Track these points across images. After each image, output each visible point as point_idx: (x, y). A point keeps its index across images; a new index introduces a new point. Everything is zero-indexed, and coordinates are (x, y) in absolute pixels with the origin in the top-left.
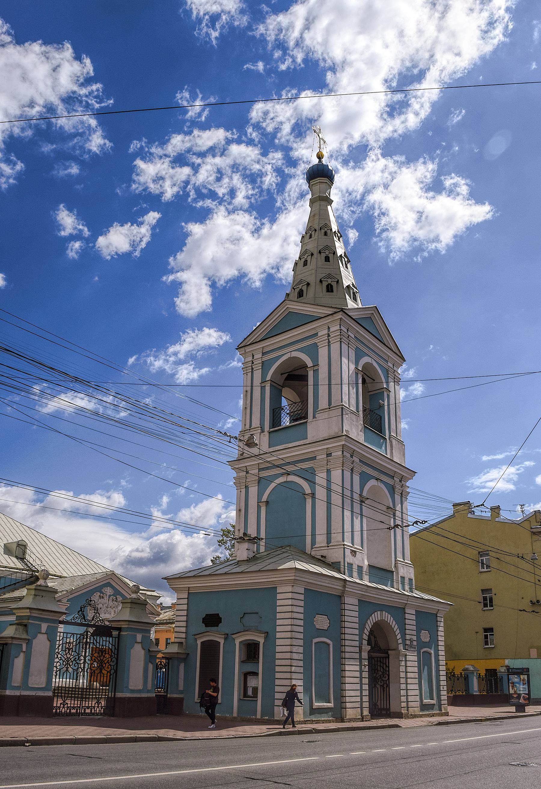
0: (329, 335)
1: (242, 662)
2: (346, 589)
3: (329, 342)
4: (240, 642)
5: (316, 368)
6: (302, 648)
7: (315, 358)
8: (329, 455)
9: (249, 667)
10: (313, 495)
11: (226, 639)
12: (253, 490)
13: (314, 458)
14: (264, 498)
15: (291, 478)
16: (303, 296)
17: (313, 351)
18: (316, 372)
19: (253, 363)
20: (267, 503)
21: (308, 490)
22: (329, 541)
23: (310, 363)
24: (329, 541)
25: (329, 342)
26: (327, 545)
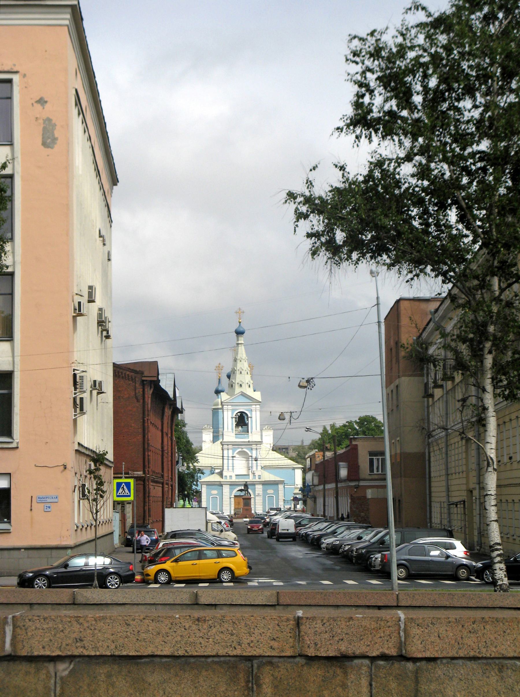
7: (251, 414)
23: (249, 416)
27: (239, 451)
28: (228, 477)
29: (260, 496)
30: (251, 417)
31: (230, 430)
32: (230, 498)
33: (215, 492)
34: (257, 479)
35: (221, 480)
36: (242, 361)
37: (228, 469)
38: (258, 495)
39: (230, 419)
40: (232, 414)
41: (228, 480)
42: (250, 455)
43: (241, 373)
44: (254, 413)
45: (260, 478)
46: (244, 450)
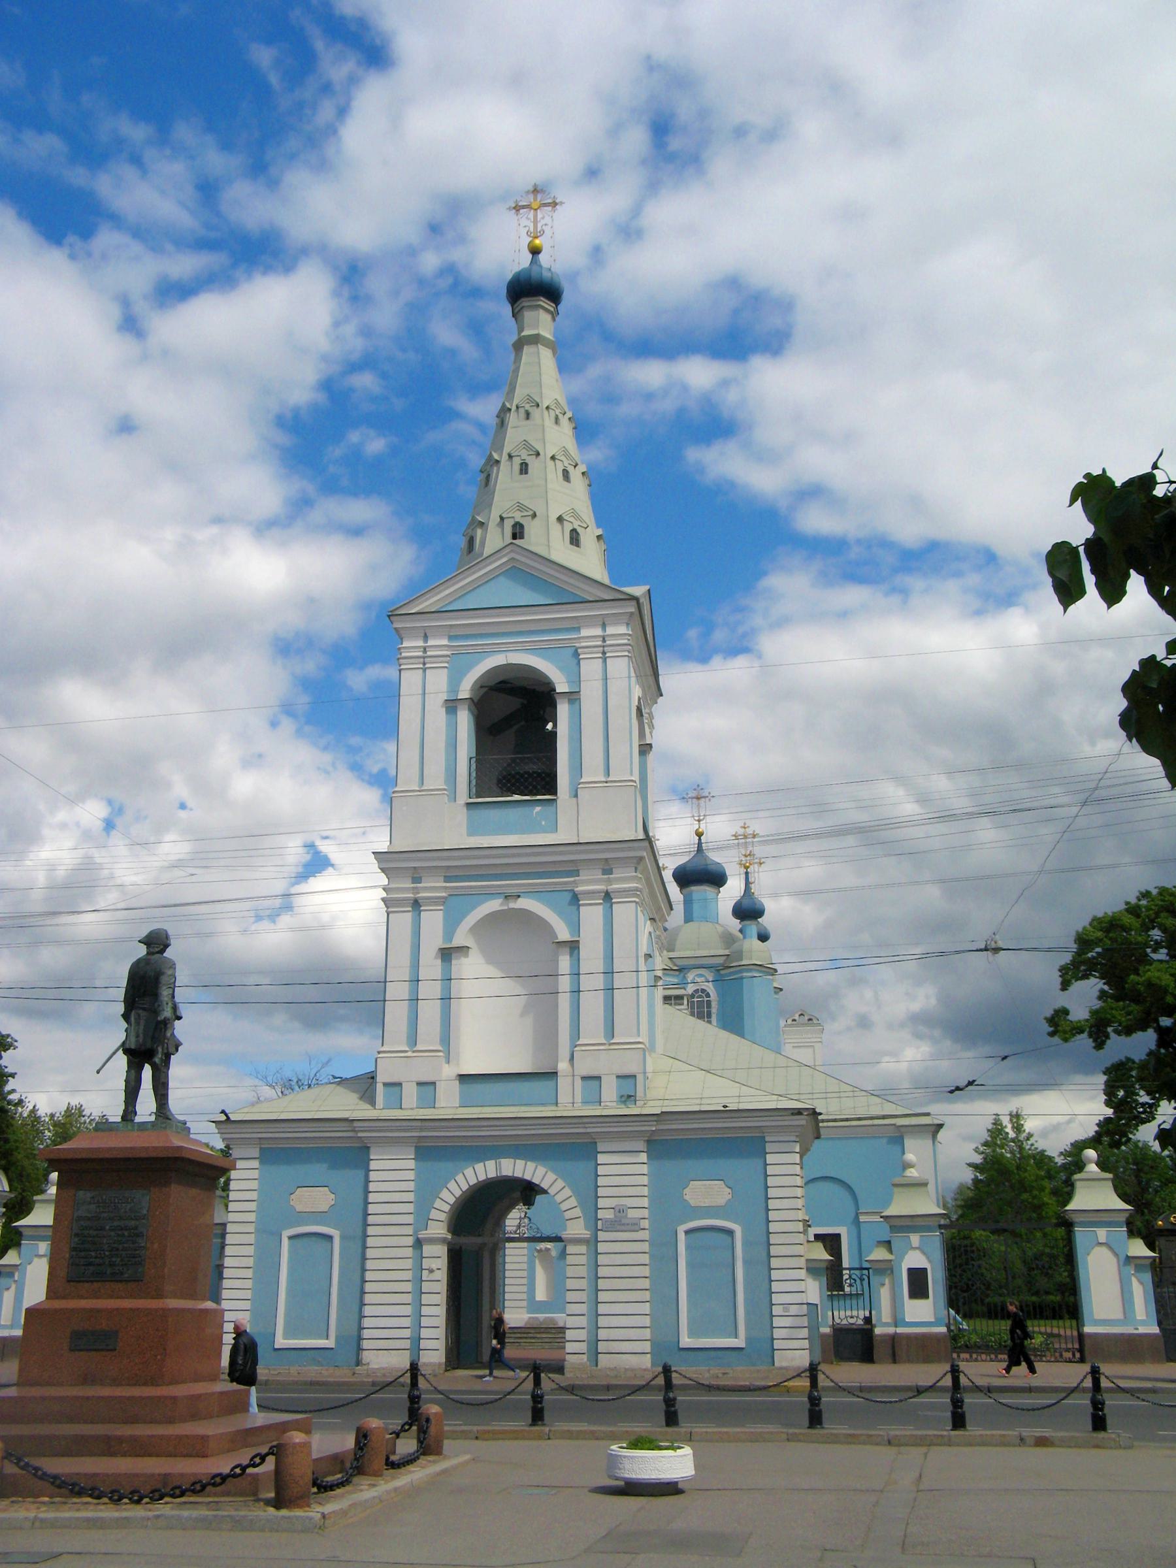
10: (573, 946)
25: (604, 653)
27: (493, 917)
28: (410, 1094)
29: (635, 1226)
30: (573, 697)
31: (436, 778)
32: (418, 1244)
33: (318, 1199)
34: (610, 1105)
35: (363, 1111)
36: (535, 413)
37: (413, 1039)
38: (620, 1223)
39: (437, 716)
40: (454, 684)
41: (411, 1107)
42: (563, 933)
43: (524, 468)
44: (591, 668)
45: (628, 1098)
46: (524, 903)
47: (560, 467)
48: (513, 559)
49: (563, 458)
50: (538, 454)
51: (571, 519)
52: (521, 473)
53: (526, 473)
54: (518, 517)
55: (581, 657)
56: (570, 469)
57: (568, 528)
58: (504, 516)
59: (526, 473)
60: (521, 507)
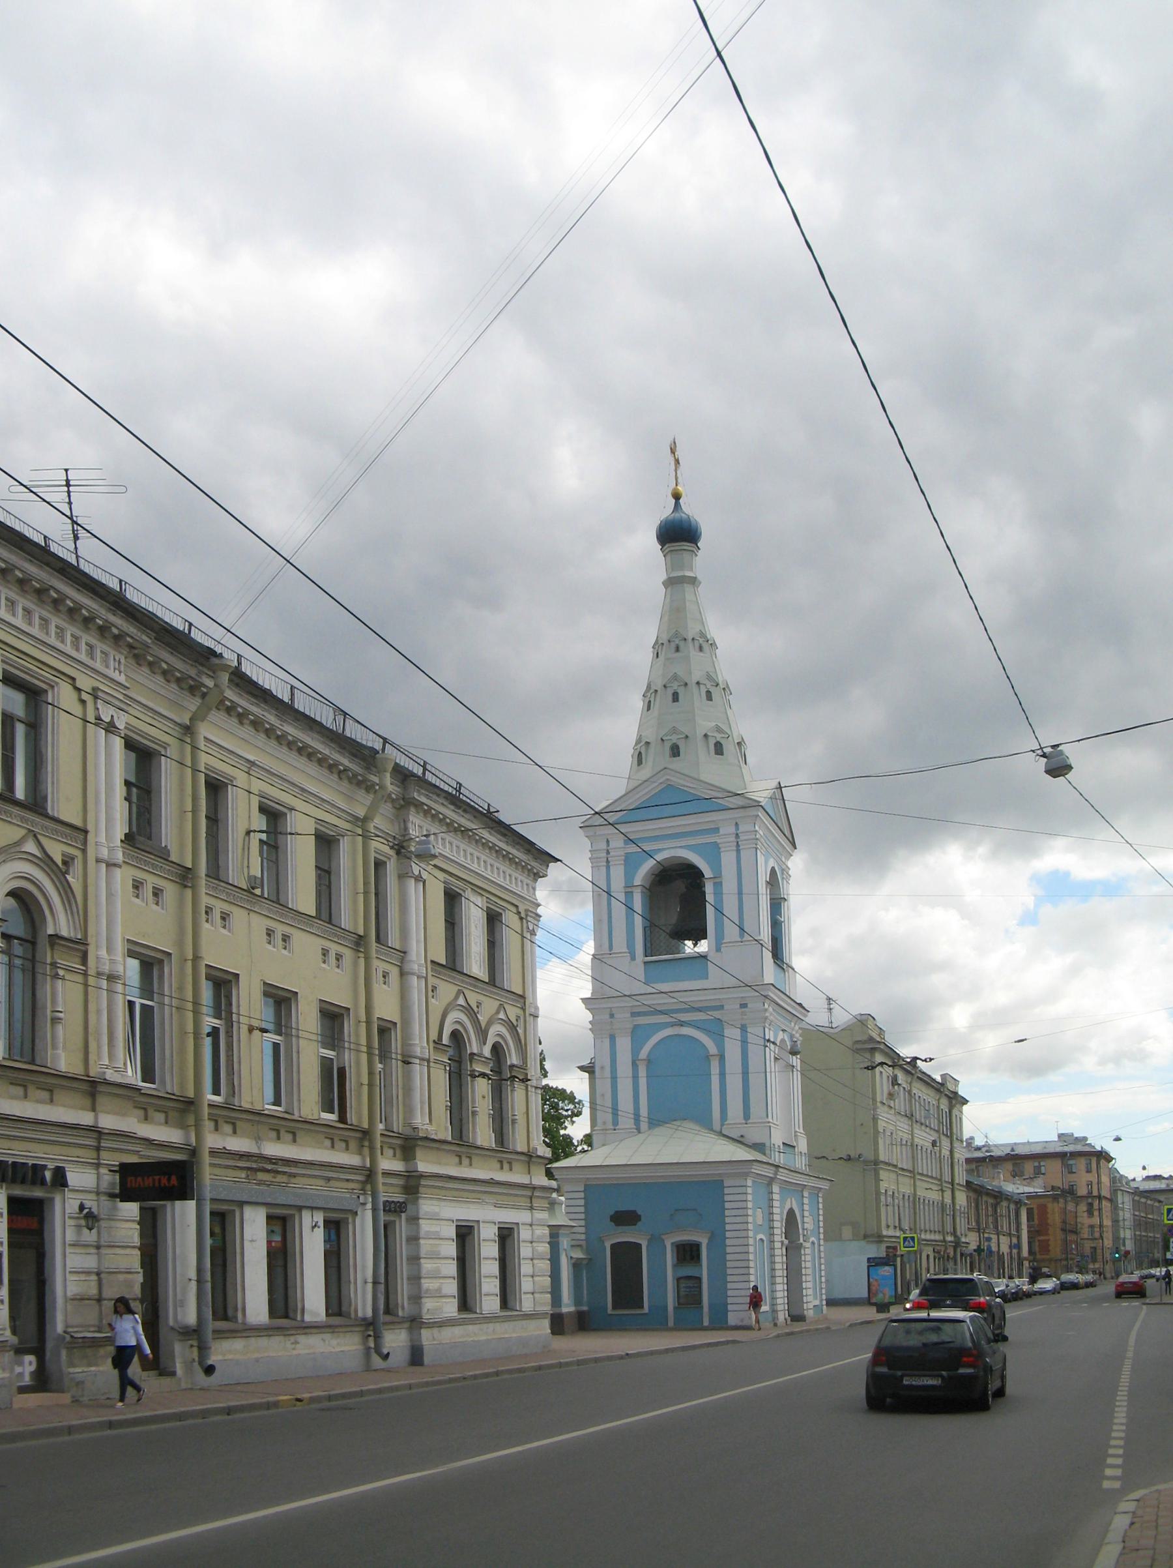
0: (737, 835)
1: (674, 1266)
2: (778, 1177)
3: (738, 845)
4: (672, 1244)
5: (717, 880)
6: (583, 1215)
8: (743, 1006)
9: (688, 1271)
10: (722, 1058)
11: (650, 1241)
12: (624, 1044)
13: (721, 1007)
14: (644, 1053)
15: (686, 1031)
16: (679, 756)
17: (713, 853)
18: (718, 885)
19: (608, 852)
20: (649, 1061)
21: (712, 1049)
22: (747, 1116)
23: (707, 873)
24: (747, 1116)
25: (738, 845)
26: (744, 1122)
46: (686, 1031)
47: (703, 690)
48: (668, 779)
49: (707, 682)
50: (686, 684)
51: (716, 734)
52: (674, 701)
53: (678, 701)
54: (674, 738)
55: (722, 850)
56: (712, 690)
57: (712, 742)
58: (664, 738)
59: (678, 701)
60: (674, 730)
